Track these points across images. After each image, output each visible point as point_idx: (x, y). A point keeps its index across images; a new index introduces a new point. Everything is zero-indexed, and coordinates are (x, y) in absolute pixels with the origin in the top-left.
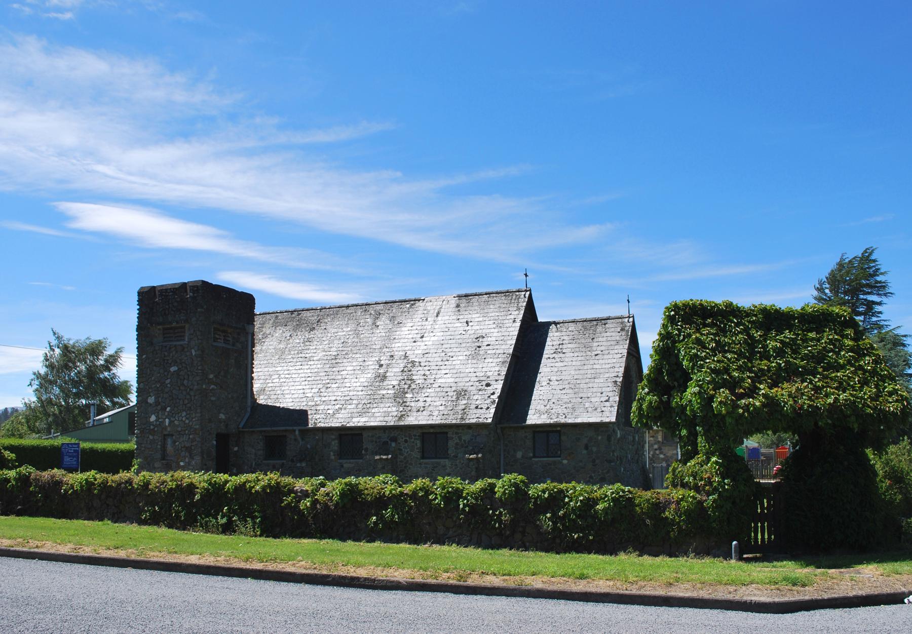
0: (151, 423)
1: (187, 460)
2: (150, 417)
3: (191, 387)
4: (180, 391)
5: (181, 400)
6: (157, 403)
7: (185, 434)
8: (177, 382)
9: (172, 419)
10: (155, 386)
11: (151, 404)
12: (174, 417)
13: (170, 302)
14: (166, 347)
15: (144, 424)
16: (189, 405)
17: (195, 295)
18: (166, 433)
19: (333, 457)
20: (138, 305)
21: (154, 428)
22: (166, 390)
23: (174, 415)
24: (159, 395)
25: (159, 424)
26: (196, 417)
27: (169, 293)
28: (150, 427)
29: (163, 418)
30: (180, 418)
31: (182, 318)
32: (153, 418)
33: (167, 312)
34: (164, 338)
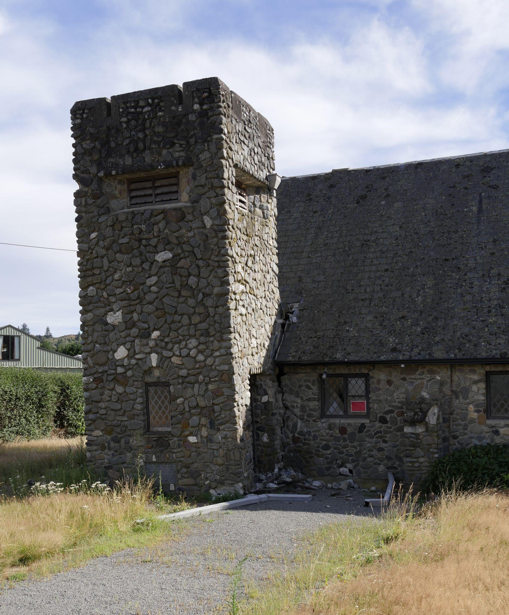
0: (116, 364)
1: (204, 432)
2: (115, 351)
3: (207, 291)
4: (181, 299)
5: (185, 317)
6: (129, 324)
7: (197, 382)
8: (173, 282)
9: (166, 353)
10: (121, 290)
11: (114, 326)
12: (171, 350)
13: (147, 125)
14: (143, 214)
15: (103, 365)
16: (204, 326)
17: (205, 107)
18: (148, 379)
19: (475, 415)
20: (72, 136)
21: (125, 373)
22: (149, 297)
23: (170, 346)
24: (132, 308)
25: (137, 364)
26: (220, 348)
27: (143, 107)
28: (115, 370)
29: (144, 353)
30: (185, 352)
31: (177, 154)
32: (121, 353)
33: (141, 145)
34: (132, 198)
